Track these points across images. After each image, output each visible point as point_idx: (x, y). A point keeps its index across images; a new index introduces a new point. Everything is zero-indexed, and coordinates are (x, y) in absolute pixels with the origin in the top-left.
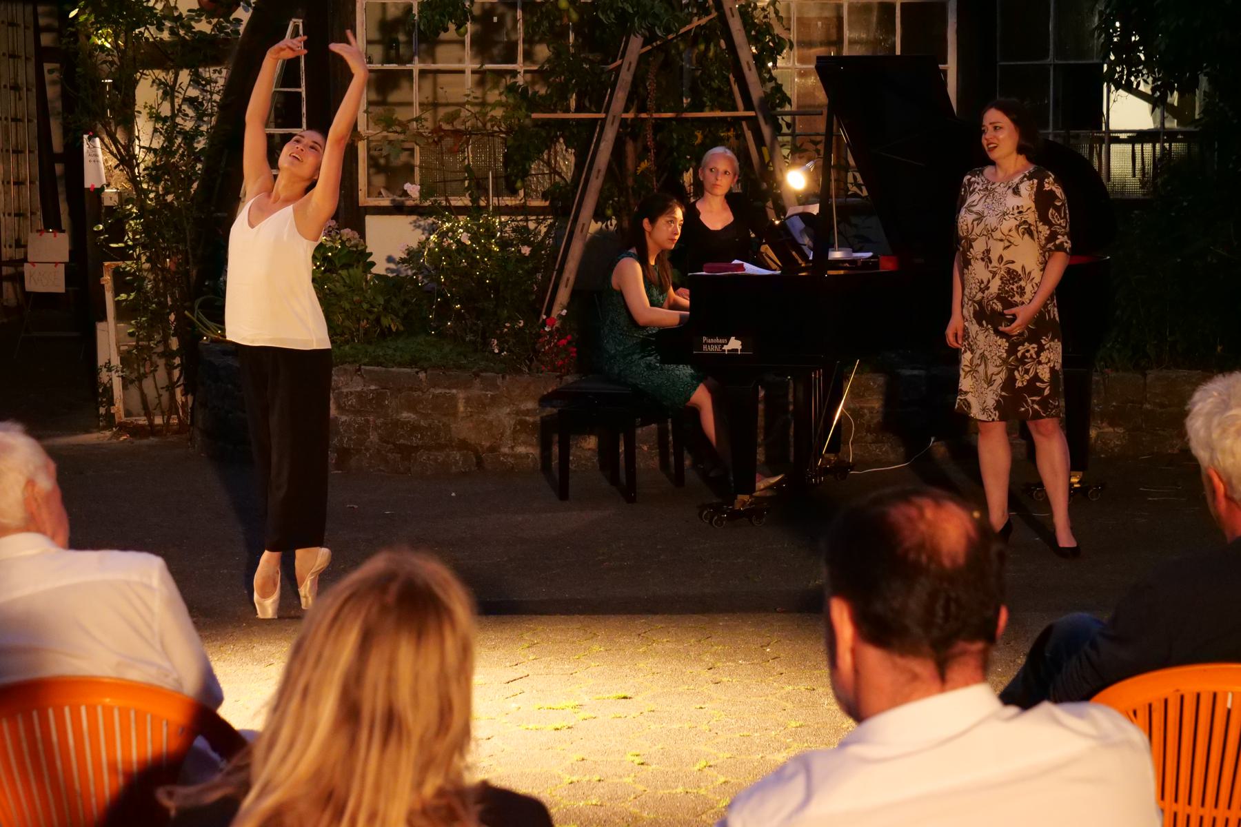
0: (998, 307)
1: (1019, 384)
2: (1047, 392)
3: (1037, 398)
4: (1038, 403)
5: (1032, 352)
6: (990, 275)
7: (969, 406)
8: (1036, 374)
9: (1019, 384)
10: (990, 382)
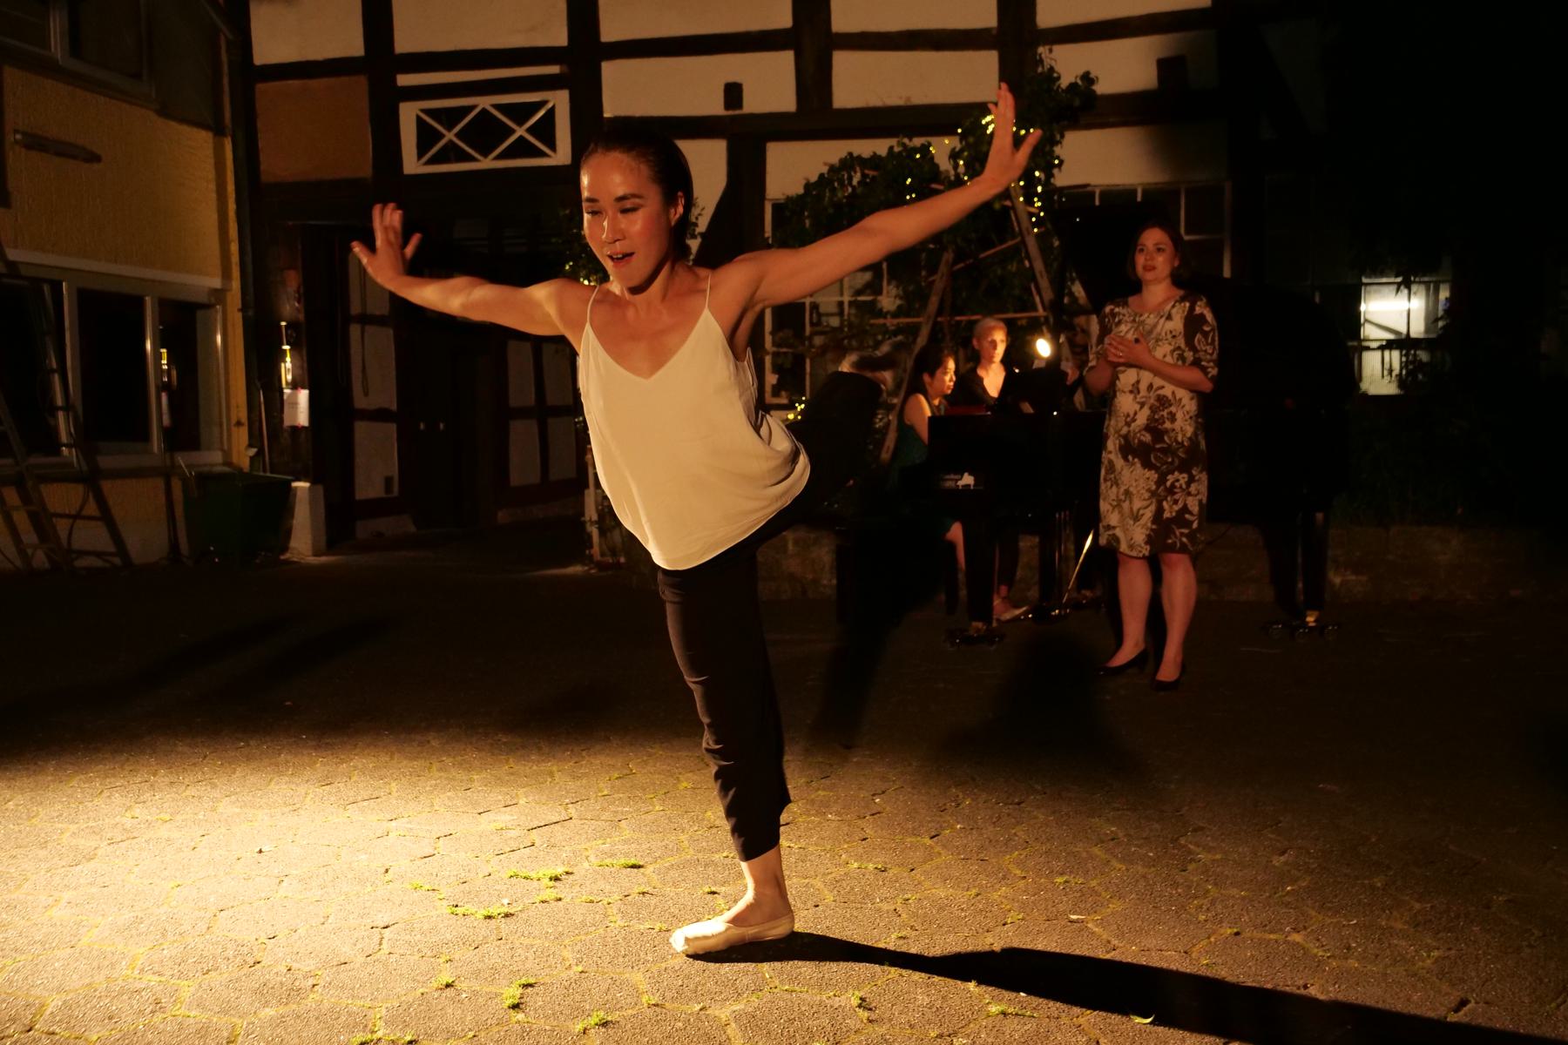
0: (1147, 438)
1: (1167, 515)
2: (1195, 525)
3: (1186, 531)
4: (1186, 536)
6: (1137, 407)
7: (1117, 540)
8: (1185, 506)
9: (1167, 515)
10: (1136, 518)
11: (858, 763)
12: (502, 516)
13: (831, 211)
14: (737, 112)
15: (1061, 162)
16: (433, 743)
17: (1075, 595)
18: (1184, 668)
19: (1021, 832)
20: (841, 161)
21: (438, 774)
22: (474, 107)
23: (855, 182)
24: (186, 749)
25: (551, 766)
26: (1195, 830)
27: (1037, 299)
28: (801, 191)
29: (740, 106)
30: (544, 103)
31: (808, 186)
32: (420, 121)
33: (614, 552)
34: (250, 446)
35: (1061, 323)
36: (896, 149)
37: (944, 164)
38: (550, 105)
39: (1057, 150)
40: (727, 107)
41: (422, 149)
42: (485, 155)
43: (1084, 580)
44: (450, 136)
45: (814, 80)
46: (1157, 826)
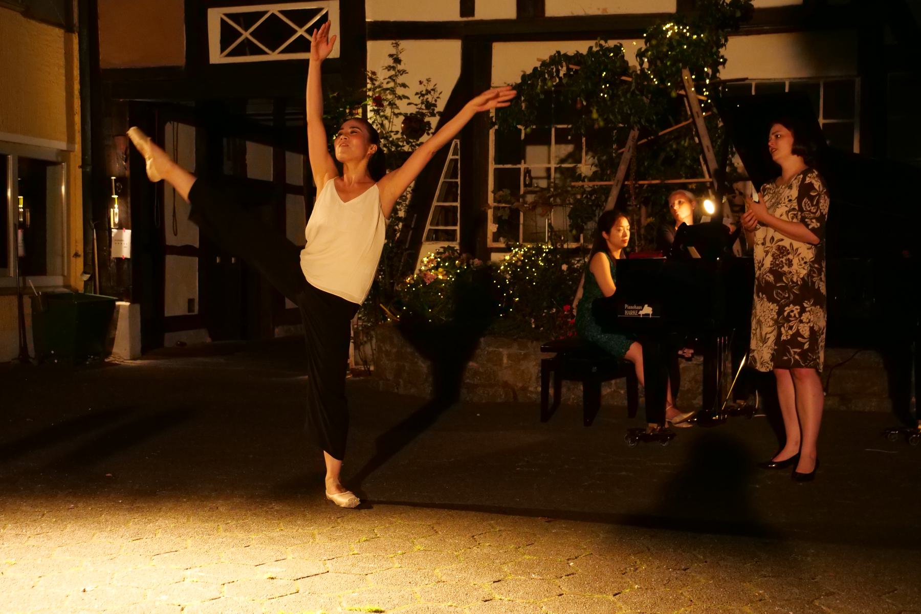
0: (771, 278)
1: (784, 338)
2: (806, 346)
3: (798, 350)
4: (799, 354)
5: (796, 312)
8: (798, 330)
9: (784, 338)
11: (556, 534)
12: (279, 332)
13: (542, 97)
14: (470, 19)
15: (725, 60)
16: (221, 509)
17: (732, 404)
18: (818, 463)
19: (686, 593)
20: (551, 57)
21: (224, 534)
22: (266, 12)
23: (561, 75)
24: (29, 509)
25: (313, 529)
26: (827, 595)
27: (705, 168)
28: (519, 81)
29: (473, 15)
30: (319, 10)
31: (524, 77)
32: (223, 22)
33: (365, 363)
34: (85, 272)
35: (724, 186)
36: (595, 49)
37: (632, 61)
38: (324, 12)
39: (722, 51)
40: (462, 15)
41: (224, 45)
42: (273, 50)
43: (739, 392)
44: (246, 34)
46: (796, 590)
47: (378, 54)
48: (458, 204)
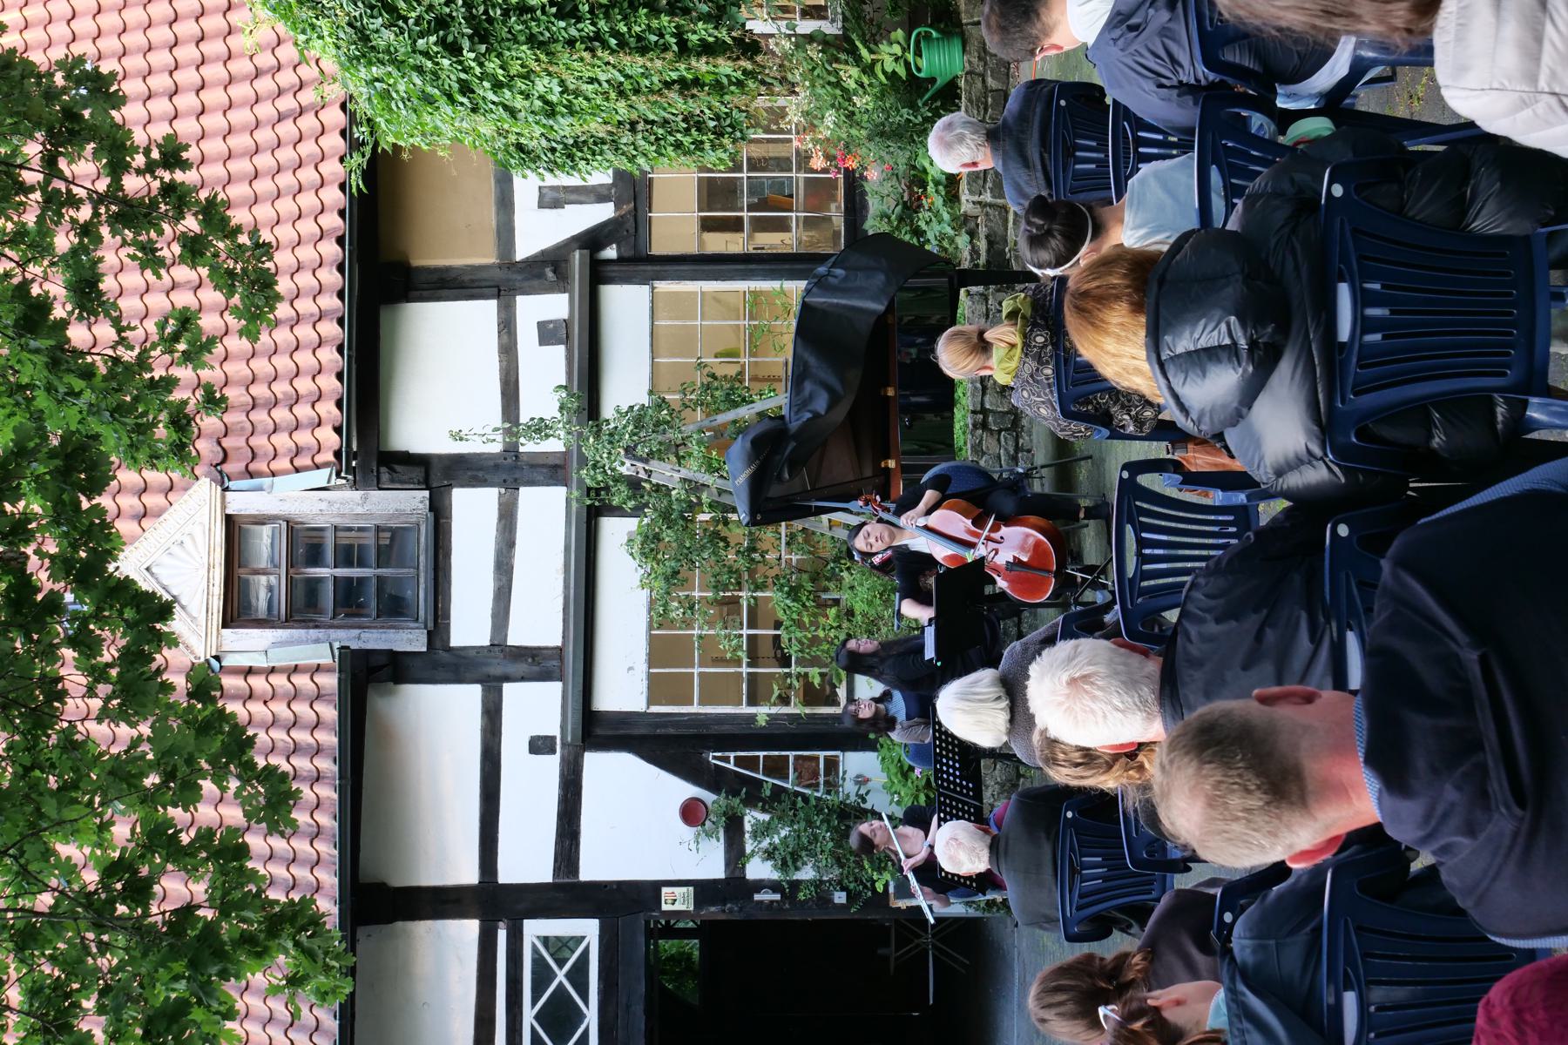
14: (558, 741)
22: (533, 1028)
29: (553, 738)
40: (553, 752)
42: (580, 1016)
45: (535, 664)
47: (594, 867)
48: (791, 754)
